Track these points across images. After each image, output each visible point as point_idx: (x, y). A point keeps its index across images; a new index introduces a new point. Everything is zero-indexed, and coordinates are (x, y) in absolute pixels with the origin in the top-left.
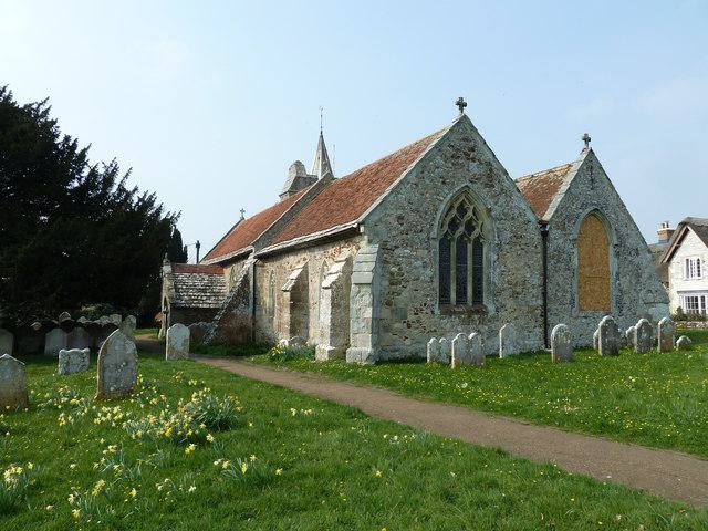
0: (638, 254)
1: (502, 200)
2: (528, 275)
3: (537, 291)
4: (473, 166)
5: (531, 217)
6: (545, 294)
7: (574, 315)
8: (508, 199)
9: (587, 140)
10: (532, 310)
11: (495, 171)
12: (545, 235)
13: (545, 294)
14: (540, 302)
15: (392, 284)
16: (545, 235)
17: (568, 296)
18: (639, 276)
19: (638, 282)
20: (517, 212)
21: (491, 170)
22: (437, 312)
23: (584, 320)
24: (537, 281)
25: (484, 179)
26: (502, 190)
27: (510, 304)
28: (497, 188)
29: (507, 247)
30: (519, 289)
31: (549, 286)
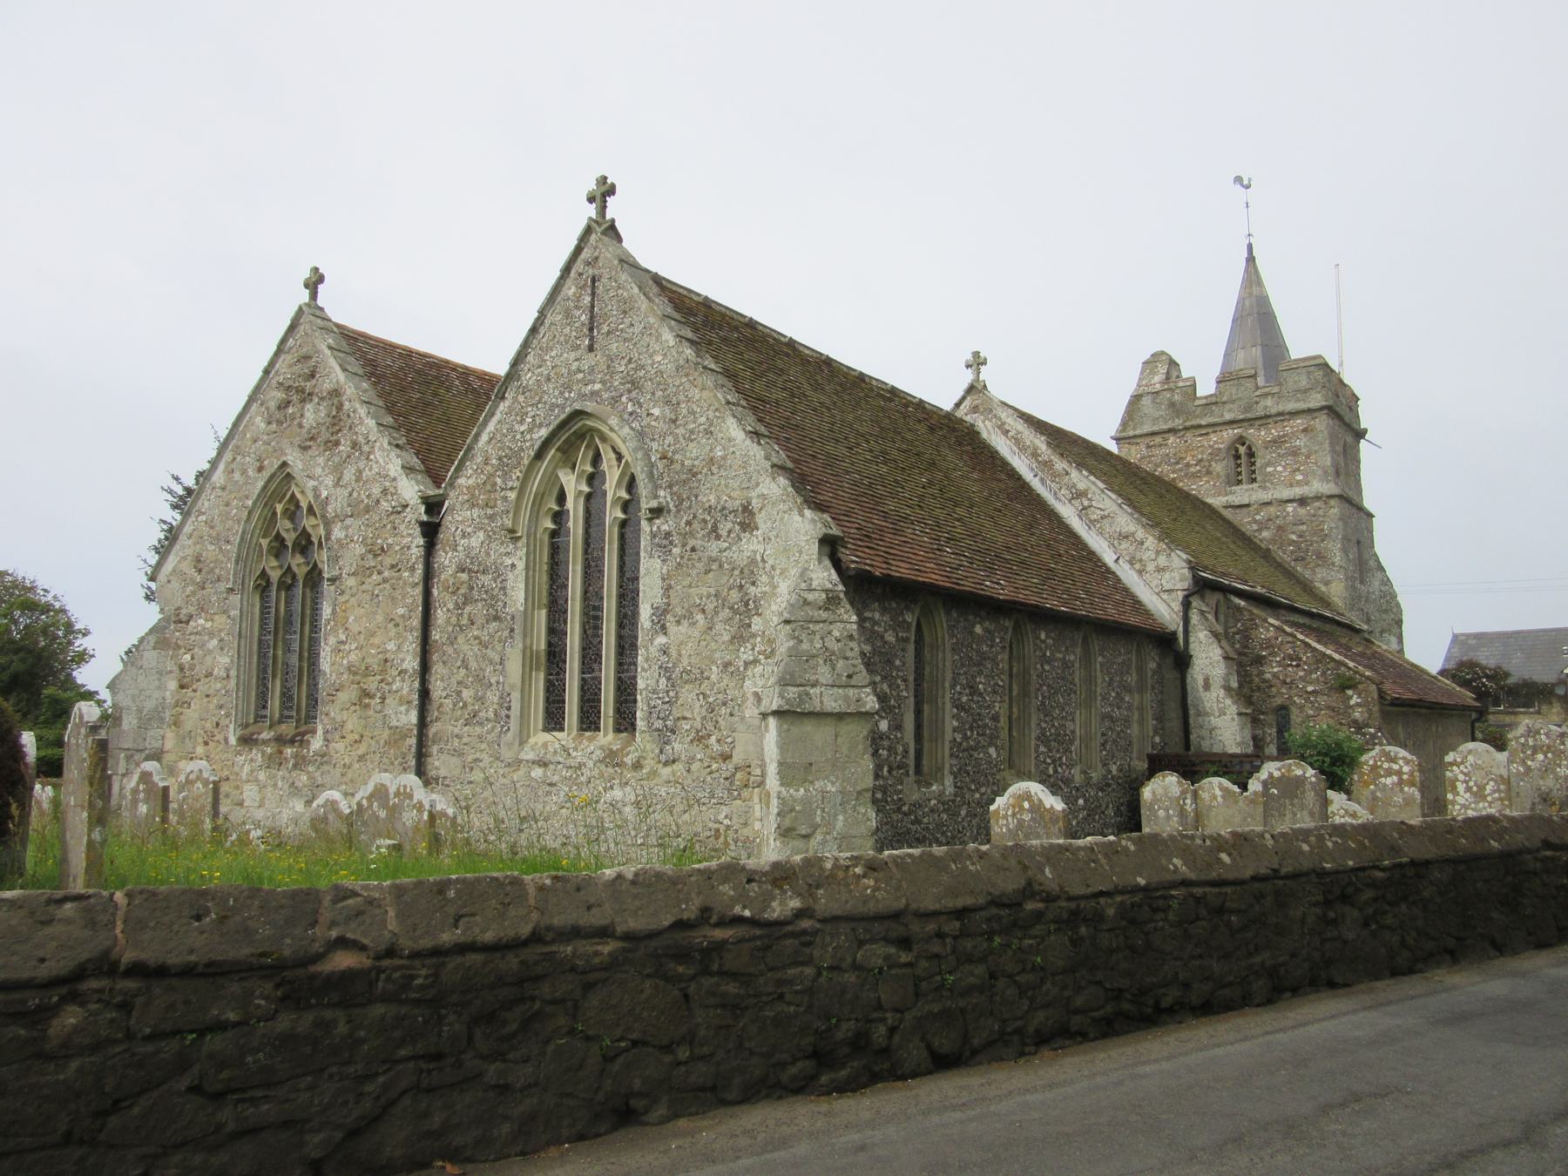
0: (748, 526)
1: (349, 474)
2: (391, 646)
3: (408, 688)
4: (312, 415)
5: (411, 490)
6: (425, 694)
7: (508, 755)
8: (361, 465)
9: (604, 192)
10: (398, 735)
11: (347, 405)
12: (431, 531)
13: (425, 694)
14: (413, 717)
15: (182, 687)
16: (431, 531)
17: (493, 697)
18: (748, 608)
19: (739, 638)
20: (376, 491)
21: (340, 407)
22: (233, 740)
23: (537, 772)
24: (412, 663)
25: (325, 435)
26: (355, 445)
27: (352, 722)
28: (344, 448)
29: (351, 582)
30: (372, 684)
31: (438, 669)
